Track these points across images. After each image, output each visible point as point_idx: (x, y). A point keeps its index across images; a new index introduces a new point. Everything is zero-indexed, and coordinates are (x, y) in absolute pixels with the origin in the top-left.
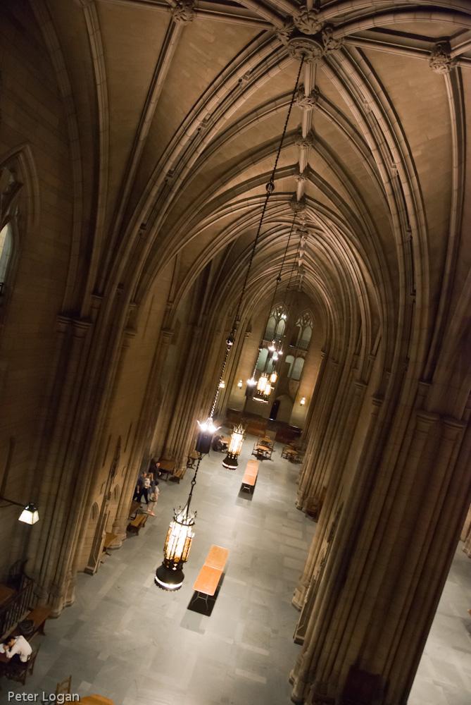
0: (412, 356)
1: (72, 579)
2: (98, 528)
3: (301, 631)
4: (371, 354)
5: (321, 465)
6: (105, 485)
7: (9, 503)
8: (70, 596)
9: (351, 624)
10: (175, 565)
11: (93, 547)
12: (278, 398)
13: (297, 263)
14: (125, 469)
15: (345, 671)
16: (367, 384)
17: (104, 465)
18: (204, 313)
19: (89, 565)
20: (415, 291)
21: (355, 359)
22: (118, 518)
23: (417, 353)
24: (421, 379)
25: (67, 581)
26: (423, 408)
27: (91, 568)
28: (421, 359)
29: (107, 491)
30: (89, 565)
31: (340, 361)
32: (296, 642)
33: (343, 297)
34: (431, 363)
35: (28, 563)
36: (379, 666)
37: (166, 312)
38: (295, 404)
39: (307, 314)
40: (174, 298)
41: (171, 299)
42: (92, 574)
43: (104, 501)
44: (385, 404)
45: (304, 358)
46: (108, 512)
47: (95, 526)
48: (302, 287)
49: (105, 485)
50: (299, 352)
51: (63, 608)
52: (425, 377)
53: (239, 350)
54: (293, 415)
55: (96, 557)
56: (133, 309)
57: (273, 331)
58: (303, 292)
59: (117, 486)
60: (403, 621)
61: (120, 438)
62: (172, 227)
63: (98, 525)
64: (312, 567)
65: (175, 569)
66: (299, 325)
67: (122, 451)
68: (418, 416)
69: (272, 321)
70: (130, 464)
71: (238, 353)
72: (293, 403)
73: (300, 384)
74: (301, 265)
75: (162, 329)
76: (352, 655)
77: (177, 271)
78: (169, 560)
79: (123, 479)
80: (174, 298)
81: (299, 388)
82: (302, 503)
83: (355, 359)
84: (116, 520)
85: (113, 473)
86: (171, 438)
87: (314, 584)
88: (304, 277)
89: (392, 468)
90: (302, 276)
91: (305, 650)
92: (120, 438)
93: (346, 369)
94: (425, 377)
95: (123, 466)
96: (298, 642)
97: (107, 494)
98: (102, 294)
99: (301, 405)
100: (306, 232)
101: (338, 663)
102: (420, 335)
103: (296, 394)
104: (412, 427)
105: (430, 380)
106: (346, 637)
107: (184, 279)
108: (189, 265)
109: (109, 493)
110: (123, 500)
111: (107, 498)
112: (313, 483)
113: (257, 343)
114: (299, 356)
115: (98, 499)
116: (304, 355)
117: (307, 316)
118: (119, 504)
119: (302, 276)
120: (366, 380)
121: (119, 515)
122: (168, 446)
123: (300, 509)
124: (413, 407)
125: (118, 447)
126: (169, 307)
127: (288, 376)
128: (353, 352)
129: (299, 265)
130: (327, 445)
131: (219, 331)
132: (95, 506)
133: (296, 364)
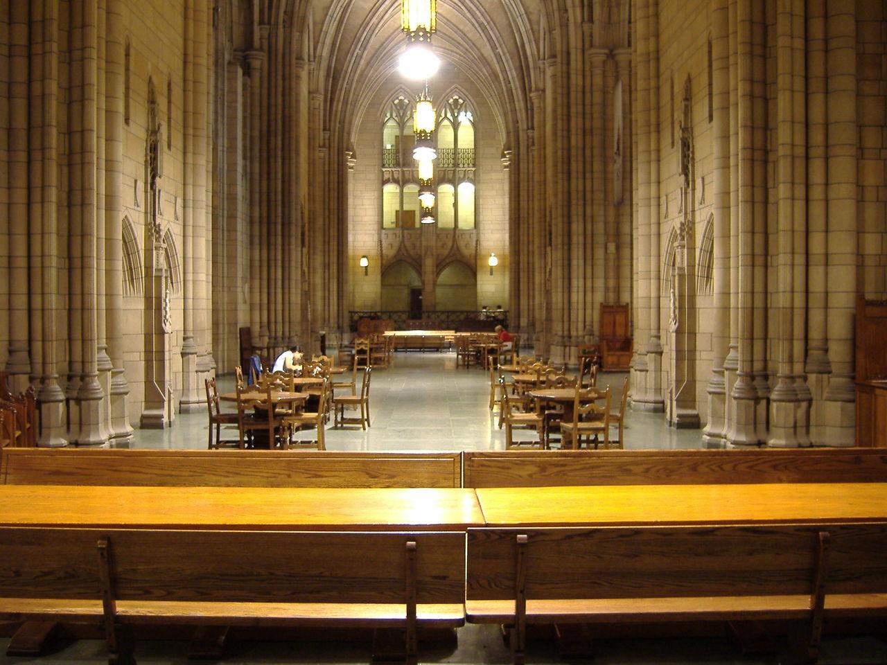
9: (817, 210)
11: (148, 362)
18: (261, 23)
19: (147, 408)
21: (587, 33)
30: (147, 408)
38: (479, 277)
39: (456, 97)
42: (160, 426)
54: (479, 294)
63: (148, 299)
72: (475, 275)
73: (478, 234)
83: (587, 33)
84: (185, 339)
93: (575, 56)
101: (816, 317)
117: (456, 101)
121: (190, 327)
128: (579, 20)
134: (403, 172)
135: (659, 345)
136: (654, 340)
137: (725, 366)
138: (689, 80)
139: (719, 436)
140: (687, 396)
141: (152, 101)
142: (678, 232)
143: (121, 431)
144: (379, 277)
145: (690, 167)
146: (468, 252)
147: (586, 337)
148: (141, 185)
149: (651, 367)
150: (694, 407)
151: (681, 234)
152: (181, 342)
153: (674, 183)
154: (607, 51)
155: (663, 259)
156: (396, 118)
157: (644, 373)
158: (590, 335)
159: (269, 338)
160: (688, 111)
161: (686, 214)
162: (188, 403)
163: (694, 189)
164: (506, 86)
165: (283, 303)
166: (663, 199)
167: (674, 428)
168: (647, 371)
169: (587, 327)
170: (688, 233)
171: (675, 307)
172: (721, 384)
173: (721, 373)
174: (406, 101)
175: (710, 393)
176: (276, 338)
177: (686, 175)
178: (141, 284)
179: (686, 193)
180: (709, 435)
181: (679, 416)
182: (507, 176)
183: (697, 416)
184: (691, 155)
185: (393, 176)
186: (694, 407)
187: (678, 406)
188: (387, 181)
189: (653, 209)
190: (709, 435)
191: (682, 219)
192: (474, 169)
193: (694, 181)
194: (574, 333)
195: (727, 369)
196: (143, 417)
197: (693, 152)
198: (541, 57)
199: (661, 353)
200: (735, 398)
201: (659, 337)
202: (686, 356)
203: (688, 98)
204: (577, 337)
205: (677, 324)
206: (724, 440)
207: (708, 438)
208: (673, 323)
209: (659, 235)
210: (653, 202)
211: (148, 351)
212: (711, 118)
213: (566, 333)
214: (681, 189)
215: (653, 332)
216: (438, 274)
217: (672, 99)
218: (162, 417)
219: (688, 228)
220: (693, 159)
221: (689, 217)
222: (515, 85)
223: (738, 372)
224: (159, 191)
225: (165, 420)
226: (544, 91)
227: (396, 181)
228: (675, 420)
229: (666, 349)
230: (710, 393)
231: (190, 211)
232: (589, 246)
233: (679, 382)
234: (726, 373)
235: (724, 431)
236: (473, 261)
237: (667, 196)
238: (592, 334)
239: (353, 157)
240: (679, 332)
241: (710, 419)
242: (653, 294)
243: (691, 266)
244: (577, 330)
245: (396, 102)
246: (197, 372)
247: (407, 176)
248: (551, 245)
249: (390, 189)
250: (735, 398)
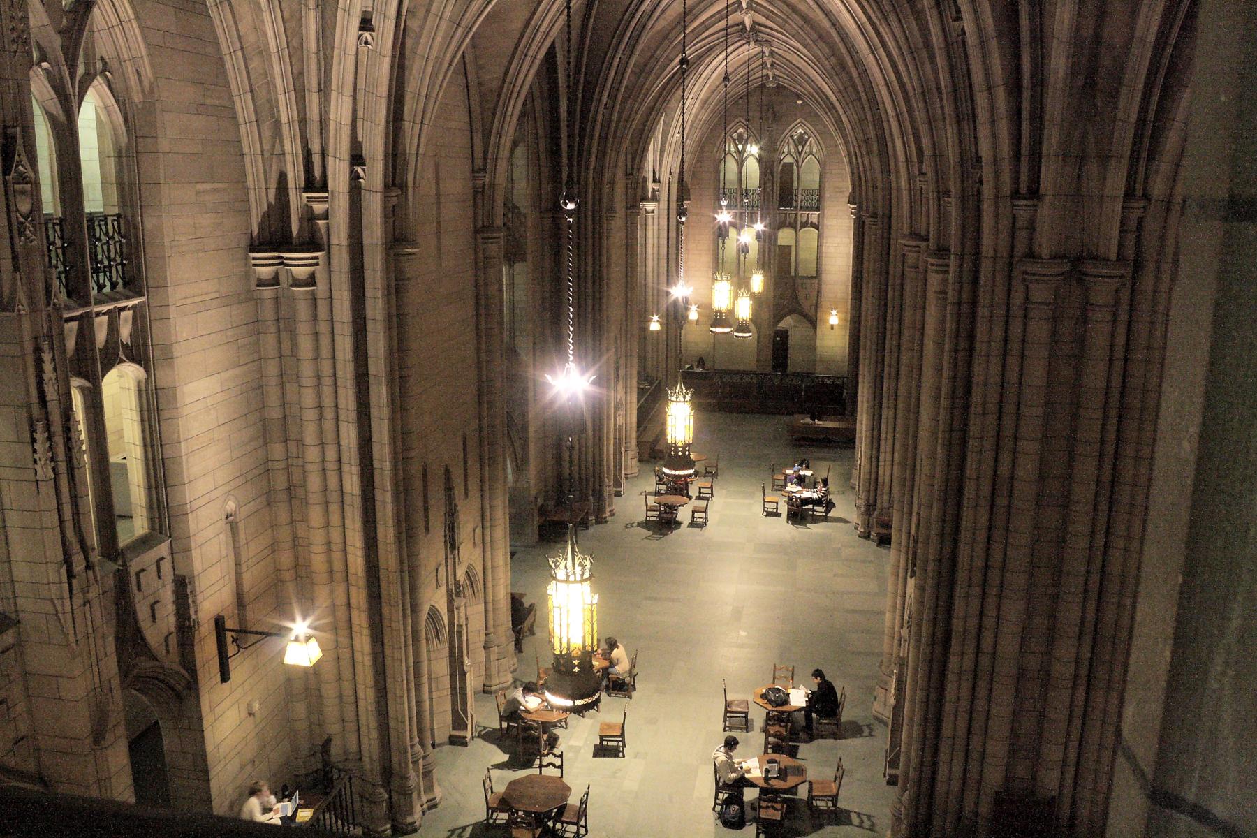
0: (985, 151)
1: (424, 757)
2: (452, 655)
3: (893, 763)
6: (442, 570)
7: (259, 637)
8: (430, 788)
10: (576, 662)
11: (454, 694)
12: (782, 325)
13: (743, 23)
14: (478, 531)
15: (985, 809)
17: (427, 529)
19: (454, 729)
20: (958, 11)
22: (492, 630)
23: (994, 139)
24: (1016, 194)
25: (415, 763)
26: (1031, 254)
27: (461, 733)
28: (1005, 150)
29: (451, 579)
30: (454, 729)
31: (880, 211)
32: (889, 783)
33: (855, 74)
34: (1027, 155)
35: (333, 743)
36: (1050, 782)
37: (476, 192)
39: (800, 130)
40: (485, 159)
41: (479, 163)
43: (450, 602)
44: (953, 261)
45: (816, 227)
46: (463, 622)
47: (446, 652)
48: (775, 75)
49: (442, 570)
50: (802, 215)
51: (424, 813)
52: (1023, 189)
55: (465, 711)
56: (394, 201)
58: (779, 87)
59: (470, 567)
60: (1081, 691)
61: (447, 471)
62: (428, 11)
63: (451, 648)
65: (576, 670)
66: (788, 160)
67: (458, 491)
68: (1025, 273)
69: (731, 164)
70: (484, 519)
73: (819, 284)
74: (752, 28)
75: (476, 231)
76: (994, 777)
77: (475, 100)
78: (561, 655)
79: (479, 551)
80: (485, 159)
82: (868, 525)
85: (452, 543)
88: (772, 53)
89: (993, 397)
90: (767, 50)
91: (904, 790)
92: (447, 471)
94: (1023, 189)
95: (470, 527)
96: (892, 781)
97: (452, 586)
98: (324, 188)
99: (832, 327)
101: (970, 797)
102: (992, 103)
103: (817, 306)
104: (1018, 298)
105: (1034, 193)
106: (976, 742)
107: (494, 114)
108: (495, 84)
109: (457, 583)
110: (490, 591)
111: (454, 593)
112: (880, 479)
114: (804, 225)
115: (435, 597)
116: (815, 220)
117: (801, 135)
118: (485, 603)
119: (767, 50)
120: (923, 233)
121: (491, 622)
123: (866, 536)
124: (1012, 257)
125: (449, 489)
126: (479, 182)
127: (792, 274)
129: (748, 28)
130: (892, 392)
131: (611, 209)
132: (434, 615)
133: (802, 243)
143: (431, 797)
146: (806, 306)
152: (483, 638)
178: (446, 638)
194: (879, 505)
196: (451, 737)
211: (453, 688)
236: (812, 313)
245: (735, 136)
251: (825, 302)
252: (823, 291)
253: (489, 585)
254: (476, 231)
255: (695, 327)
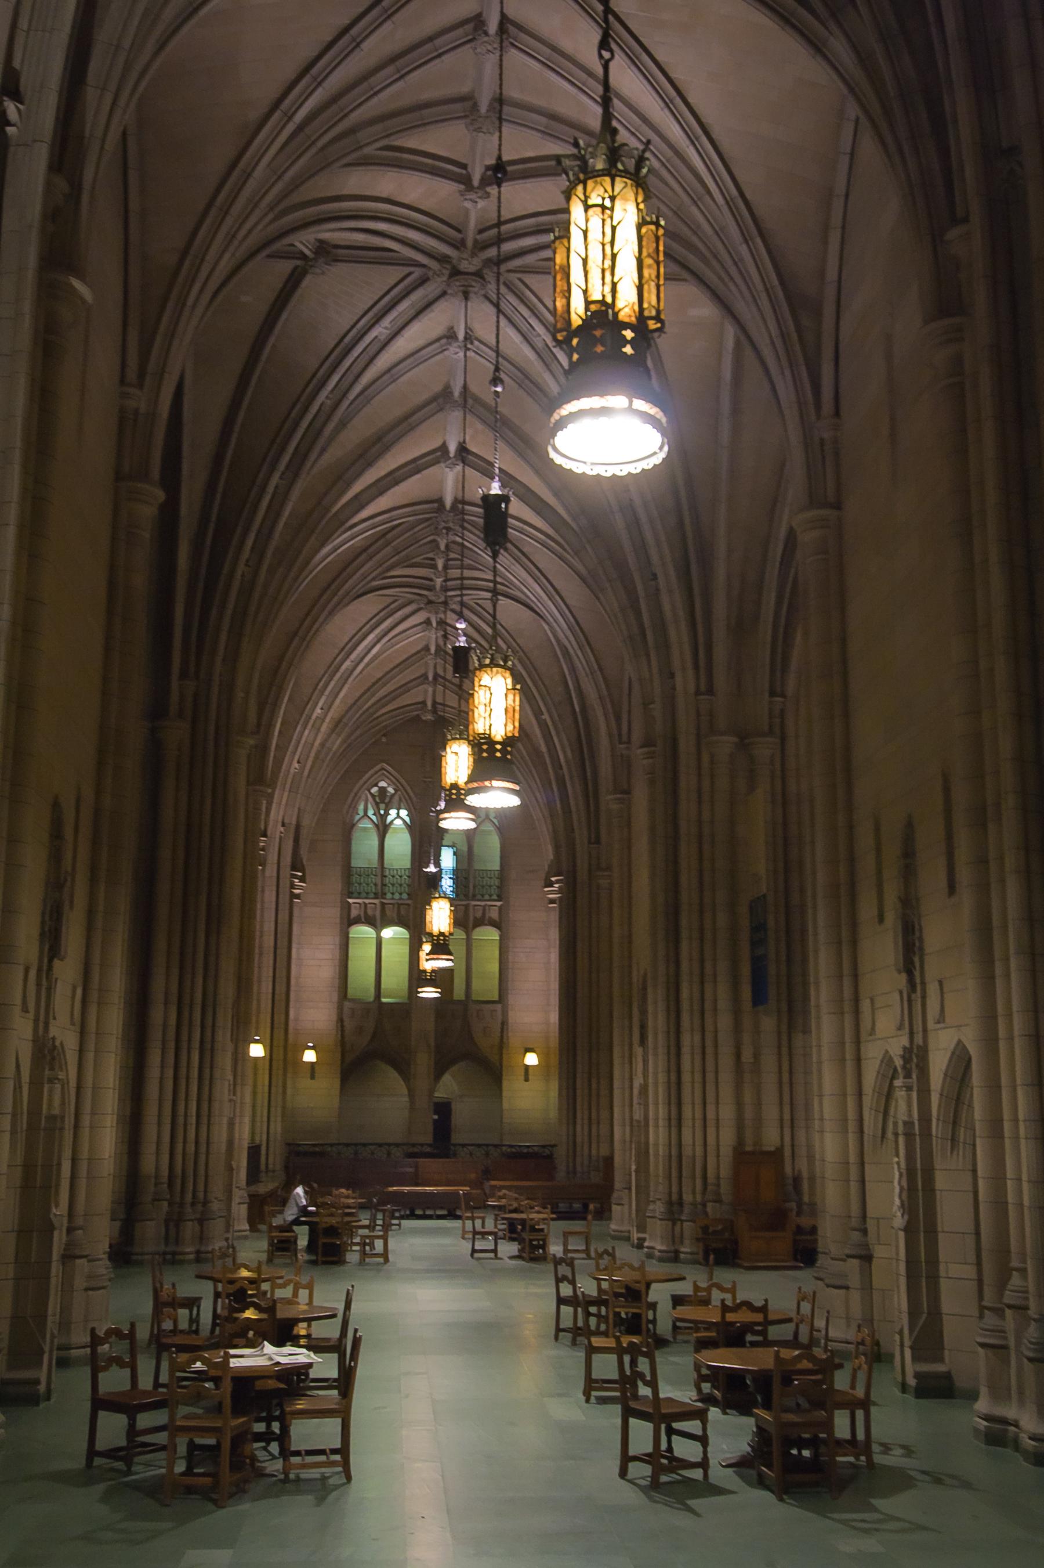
4: (819, 416)
5: (698, 1077)
12: (440, 1094)
16: (838, 506)
18: (184, 675)
22: (79, 1221)
38: (505, 1083)
40: (142, 374)
41: (132, 374)
53: (283, 928)
57: (375, 863)
64: (854, 1175)
71: (283, 942)
73: (505, 1013)
80: (142, 374)
81: (504, 1024)
86: (150, 1131)
87: (909, 1136)
93: (686, 744)
100: (479, 274)
103: (502, 1045)
113: (334, 913)
114: (479, 923)
116: (494, 914)
122: (148, 1163)
128: (692, 688)
134: (383, 904)
135: (866, 1246)
136: (856, 1236)
137: (1006, 1300)
138: (910, 825)
139: (1004, 1421)
140: (928, 1339)
141: (56, 834)
142: (898, 1062)
144: (337, 1083)
145: (916, 959)
147: (710, 1205)
148: (33, 974)
149: (854, 1280)
150: (941, 1360)
151: (904, 1067)
153: (883, 979)
154: (735, 739)
155: (867, 1101)
156: (374, 818)
157: (842, 1292)
158: (715, 1201)
159: (170, 1205)
160: (909, 872)
161: (912, 1034)
162: (68, 1348)
163: (924, 997)
164: (556, 773)
165: (197, 1142)
166: (865, 1005)
167: (910, 1398)
168: (847, 1288)
169: (710, 1188)
170: (917, 1066)
171: (902, 1189)
172: (1001, 1332)
173: (999, 1312)
174: (391, 790)
175: (983, 1345)
176: (182, 1204)
177: (910, 973)
179: (910, 1001)
180: (987, 1418)
181: (917, 1375)
182: (554, 917)
183: (948, 1376)
184: (917, 944)
185: (365, 912)
186: (941, 1360)
187: (915, 1359)
188: (357, 921)
189: (848, 1019)
190: (987, 1418)
191: (905, 1041)
192: (499, 904)
193: (923, 983)
195: (1010, 1307)
197: (921, 940)
198: (625, 738)
199: (867, 1258)
200: (1030, 1360)
201: (865, 1232)
202: (922, 1272)
203: (908, 853)
204: (694, 1204)
205: (906, 1217)
206: (1012, 1428)
207: (985, 1423)
208: (899, 1214)
209: (858, 1060)
210: (847, 1007)
212: (952, 888)
213: (675, 1197)
214: (901, 992)
215: (855, 1222)
216: (438, 1077)
217: (878, 850)
218: (37, 1382)
219: (916, 1057)
220: (921, 949)
221: (919, 1039)
222: (570, 771)
223: (1030, 1312)
224: (56, 979)
225: (42, 1388)
226: (628, 792)
227: (370, 922)
228: (912, 1382)
229: (880, 1252)
230: (983, 1345)
231: (93, 1010)
232: (709, 1050)
233: (914, 1313)
234: (1008, 1312)
235: (1010, 1412)
237: (872, 1000)
238: (718, 1201)
239: (302, 879)
240: (909, 1230)
241: (984, 1391)
242: (853, 1158)
243: (925, 1119)
244: (694, 1193)
245: (374, 790)
246: (87, 1289)
247: (388, 913)
248: (643, 1041)
249: (363, 932)
250: (1030, 1360)
251: (514, 1041)
252: (510, 1021)
253: (86, 1120)
254: (119, 476)
255: (305, 1083)
